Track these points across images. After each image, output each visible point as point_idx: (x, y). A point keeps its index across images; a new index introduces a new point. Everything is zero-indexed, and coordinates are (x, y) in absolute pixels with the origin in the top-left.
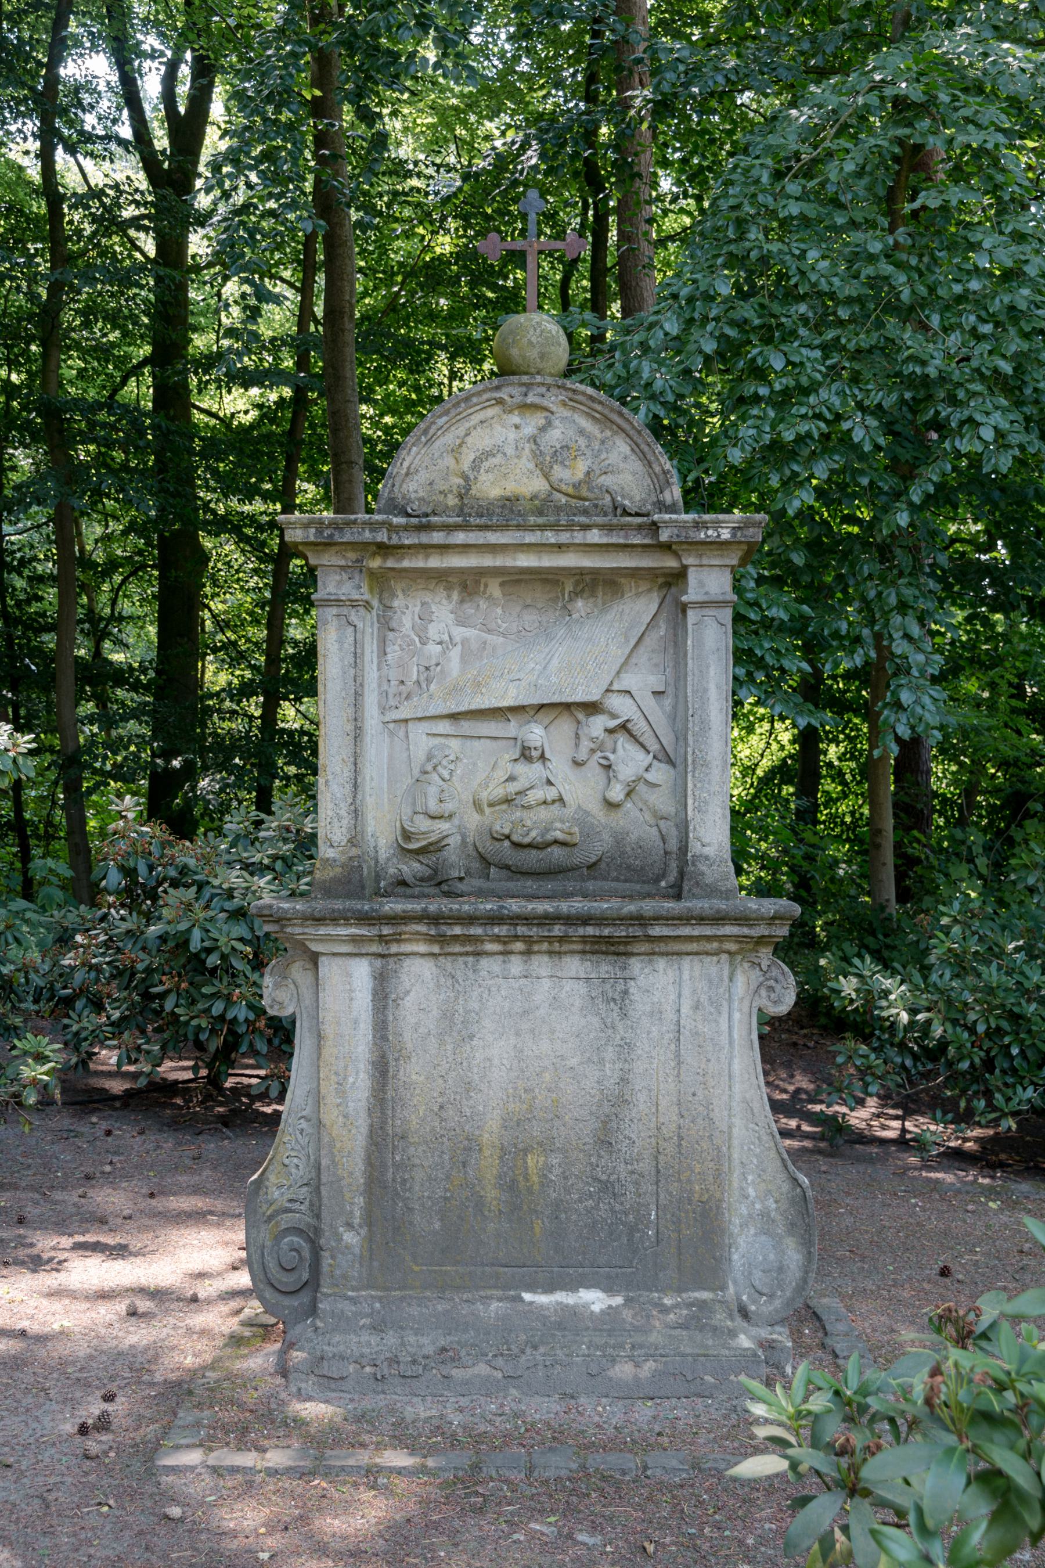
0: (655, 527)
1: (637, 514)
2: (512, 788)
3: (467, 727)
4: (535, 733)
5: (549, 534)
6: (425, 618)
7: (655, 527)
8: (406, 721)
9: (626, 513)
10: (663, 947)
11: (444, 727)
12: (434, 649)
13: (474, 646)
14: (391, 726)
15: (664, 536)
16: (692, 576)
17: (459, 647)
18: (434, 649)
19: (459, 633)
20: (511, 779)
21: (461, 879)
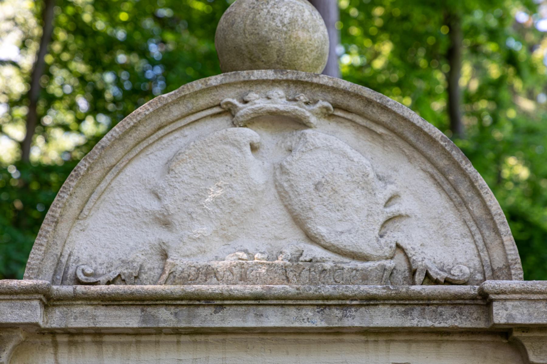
0: (484, 301)
1: (447, 282)
7: (484, 301)
9: (429, 279)
15: (501, 315)
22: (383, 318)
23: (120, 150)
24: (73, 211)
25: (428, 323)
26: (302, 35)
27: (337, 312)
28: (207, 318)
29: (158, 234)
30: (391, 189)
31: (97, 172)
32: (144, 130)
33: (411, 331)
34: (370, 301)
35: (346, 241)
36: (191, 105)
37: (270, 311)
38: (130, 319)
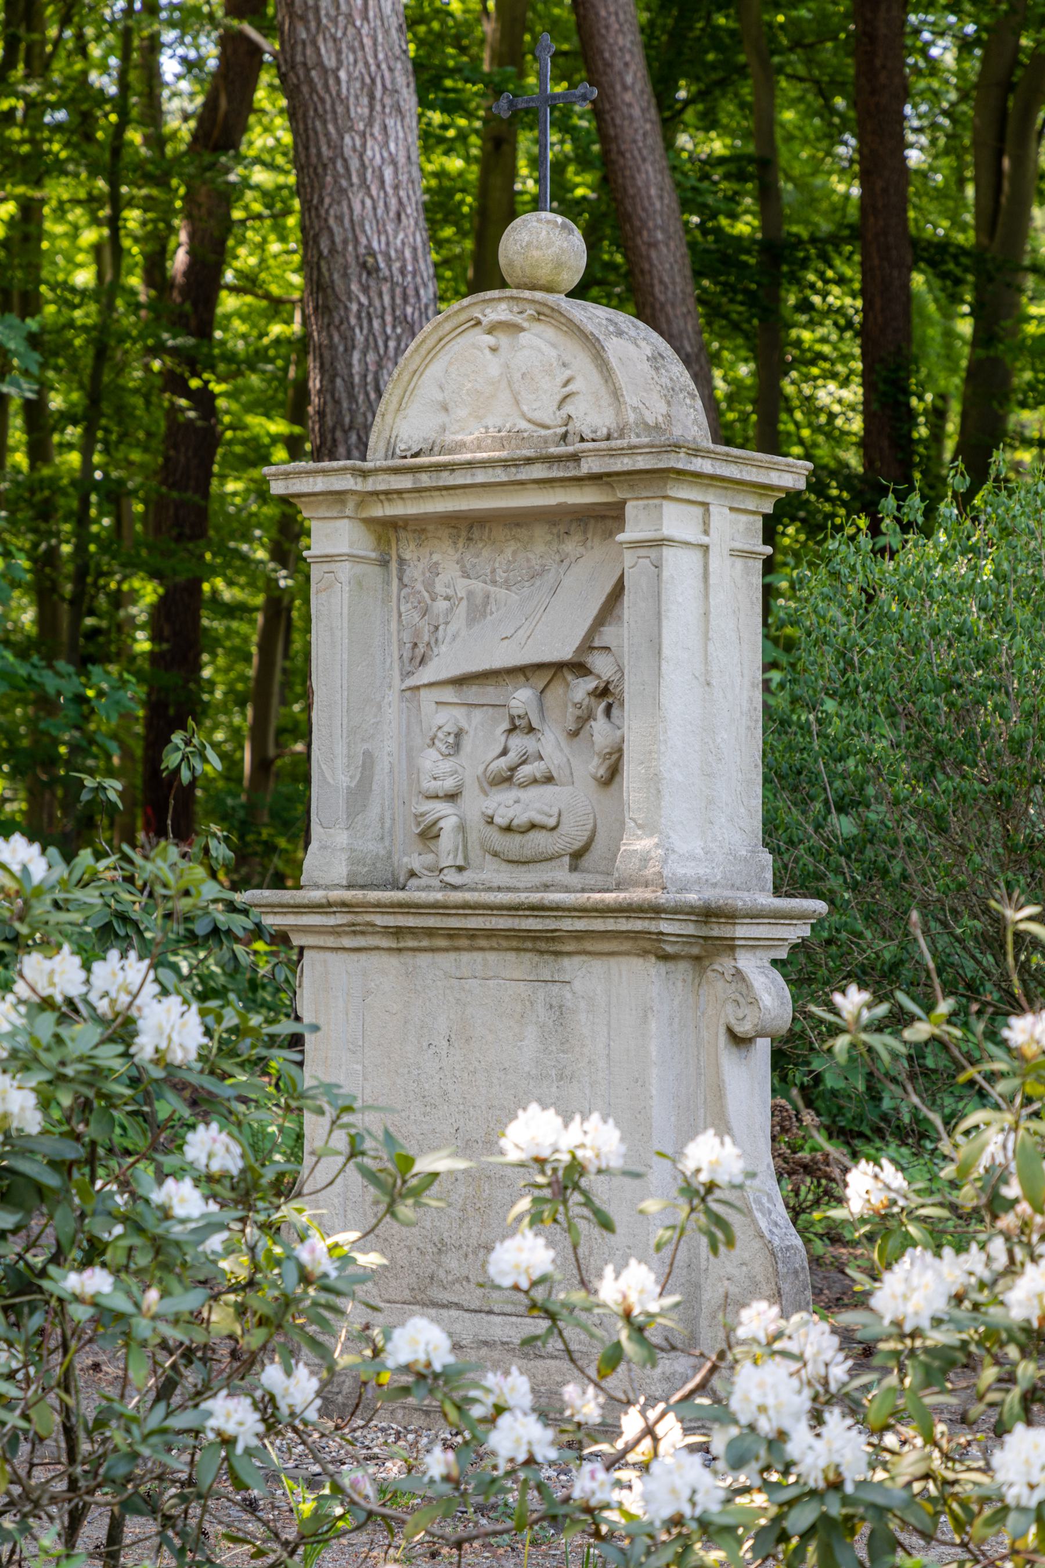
2: (503, 763)
3: (472, 694)
4: (522, 698)
5: (499, 471)
6: (434, 570)
8: (418, 688)
10: (588, 946)
11: (448, 694)
12: (442, 605)
13: (479, 601)
14: (408, 694)
16: (630, 509)
17: (464, 603)
18: (442, 605)
19: (462, 586)
20: (504, 753)
21: (460, 869)
22: (538, 472)
23: (417, 360)
24: (393, 406)
25: (561, 474)
26: (536, 253)
27: (513, 470)
28: (447, 479)
29: (442, 418)
30: (568, 373)
31: (406, 377)
32: (430, 343)
33: (562, 480)
34: (529, 461)
35: (537, 416)
36: (455, 321)
37: (478, 471)
38: (405, 482)
